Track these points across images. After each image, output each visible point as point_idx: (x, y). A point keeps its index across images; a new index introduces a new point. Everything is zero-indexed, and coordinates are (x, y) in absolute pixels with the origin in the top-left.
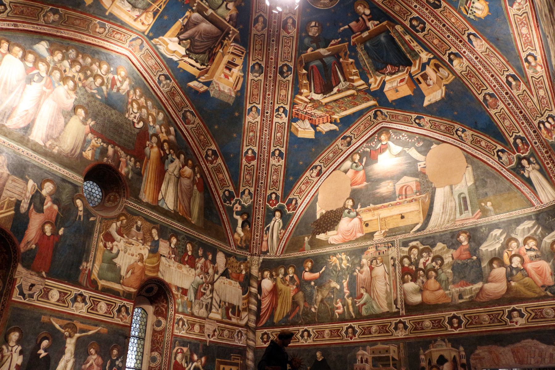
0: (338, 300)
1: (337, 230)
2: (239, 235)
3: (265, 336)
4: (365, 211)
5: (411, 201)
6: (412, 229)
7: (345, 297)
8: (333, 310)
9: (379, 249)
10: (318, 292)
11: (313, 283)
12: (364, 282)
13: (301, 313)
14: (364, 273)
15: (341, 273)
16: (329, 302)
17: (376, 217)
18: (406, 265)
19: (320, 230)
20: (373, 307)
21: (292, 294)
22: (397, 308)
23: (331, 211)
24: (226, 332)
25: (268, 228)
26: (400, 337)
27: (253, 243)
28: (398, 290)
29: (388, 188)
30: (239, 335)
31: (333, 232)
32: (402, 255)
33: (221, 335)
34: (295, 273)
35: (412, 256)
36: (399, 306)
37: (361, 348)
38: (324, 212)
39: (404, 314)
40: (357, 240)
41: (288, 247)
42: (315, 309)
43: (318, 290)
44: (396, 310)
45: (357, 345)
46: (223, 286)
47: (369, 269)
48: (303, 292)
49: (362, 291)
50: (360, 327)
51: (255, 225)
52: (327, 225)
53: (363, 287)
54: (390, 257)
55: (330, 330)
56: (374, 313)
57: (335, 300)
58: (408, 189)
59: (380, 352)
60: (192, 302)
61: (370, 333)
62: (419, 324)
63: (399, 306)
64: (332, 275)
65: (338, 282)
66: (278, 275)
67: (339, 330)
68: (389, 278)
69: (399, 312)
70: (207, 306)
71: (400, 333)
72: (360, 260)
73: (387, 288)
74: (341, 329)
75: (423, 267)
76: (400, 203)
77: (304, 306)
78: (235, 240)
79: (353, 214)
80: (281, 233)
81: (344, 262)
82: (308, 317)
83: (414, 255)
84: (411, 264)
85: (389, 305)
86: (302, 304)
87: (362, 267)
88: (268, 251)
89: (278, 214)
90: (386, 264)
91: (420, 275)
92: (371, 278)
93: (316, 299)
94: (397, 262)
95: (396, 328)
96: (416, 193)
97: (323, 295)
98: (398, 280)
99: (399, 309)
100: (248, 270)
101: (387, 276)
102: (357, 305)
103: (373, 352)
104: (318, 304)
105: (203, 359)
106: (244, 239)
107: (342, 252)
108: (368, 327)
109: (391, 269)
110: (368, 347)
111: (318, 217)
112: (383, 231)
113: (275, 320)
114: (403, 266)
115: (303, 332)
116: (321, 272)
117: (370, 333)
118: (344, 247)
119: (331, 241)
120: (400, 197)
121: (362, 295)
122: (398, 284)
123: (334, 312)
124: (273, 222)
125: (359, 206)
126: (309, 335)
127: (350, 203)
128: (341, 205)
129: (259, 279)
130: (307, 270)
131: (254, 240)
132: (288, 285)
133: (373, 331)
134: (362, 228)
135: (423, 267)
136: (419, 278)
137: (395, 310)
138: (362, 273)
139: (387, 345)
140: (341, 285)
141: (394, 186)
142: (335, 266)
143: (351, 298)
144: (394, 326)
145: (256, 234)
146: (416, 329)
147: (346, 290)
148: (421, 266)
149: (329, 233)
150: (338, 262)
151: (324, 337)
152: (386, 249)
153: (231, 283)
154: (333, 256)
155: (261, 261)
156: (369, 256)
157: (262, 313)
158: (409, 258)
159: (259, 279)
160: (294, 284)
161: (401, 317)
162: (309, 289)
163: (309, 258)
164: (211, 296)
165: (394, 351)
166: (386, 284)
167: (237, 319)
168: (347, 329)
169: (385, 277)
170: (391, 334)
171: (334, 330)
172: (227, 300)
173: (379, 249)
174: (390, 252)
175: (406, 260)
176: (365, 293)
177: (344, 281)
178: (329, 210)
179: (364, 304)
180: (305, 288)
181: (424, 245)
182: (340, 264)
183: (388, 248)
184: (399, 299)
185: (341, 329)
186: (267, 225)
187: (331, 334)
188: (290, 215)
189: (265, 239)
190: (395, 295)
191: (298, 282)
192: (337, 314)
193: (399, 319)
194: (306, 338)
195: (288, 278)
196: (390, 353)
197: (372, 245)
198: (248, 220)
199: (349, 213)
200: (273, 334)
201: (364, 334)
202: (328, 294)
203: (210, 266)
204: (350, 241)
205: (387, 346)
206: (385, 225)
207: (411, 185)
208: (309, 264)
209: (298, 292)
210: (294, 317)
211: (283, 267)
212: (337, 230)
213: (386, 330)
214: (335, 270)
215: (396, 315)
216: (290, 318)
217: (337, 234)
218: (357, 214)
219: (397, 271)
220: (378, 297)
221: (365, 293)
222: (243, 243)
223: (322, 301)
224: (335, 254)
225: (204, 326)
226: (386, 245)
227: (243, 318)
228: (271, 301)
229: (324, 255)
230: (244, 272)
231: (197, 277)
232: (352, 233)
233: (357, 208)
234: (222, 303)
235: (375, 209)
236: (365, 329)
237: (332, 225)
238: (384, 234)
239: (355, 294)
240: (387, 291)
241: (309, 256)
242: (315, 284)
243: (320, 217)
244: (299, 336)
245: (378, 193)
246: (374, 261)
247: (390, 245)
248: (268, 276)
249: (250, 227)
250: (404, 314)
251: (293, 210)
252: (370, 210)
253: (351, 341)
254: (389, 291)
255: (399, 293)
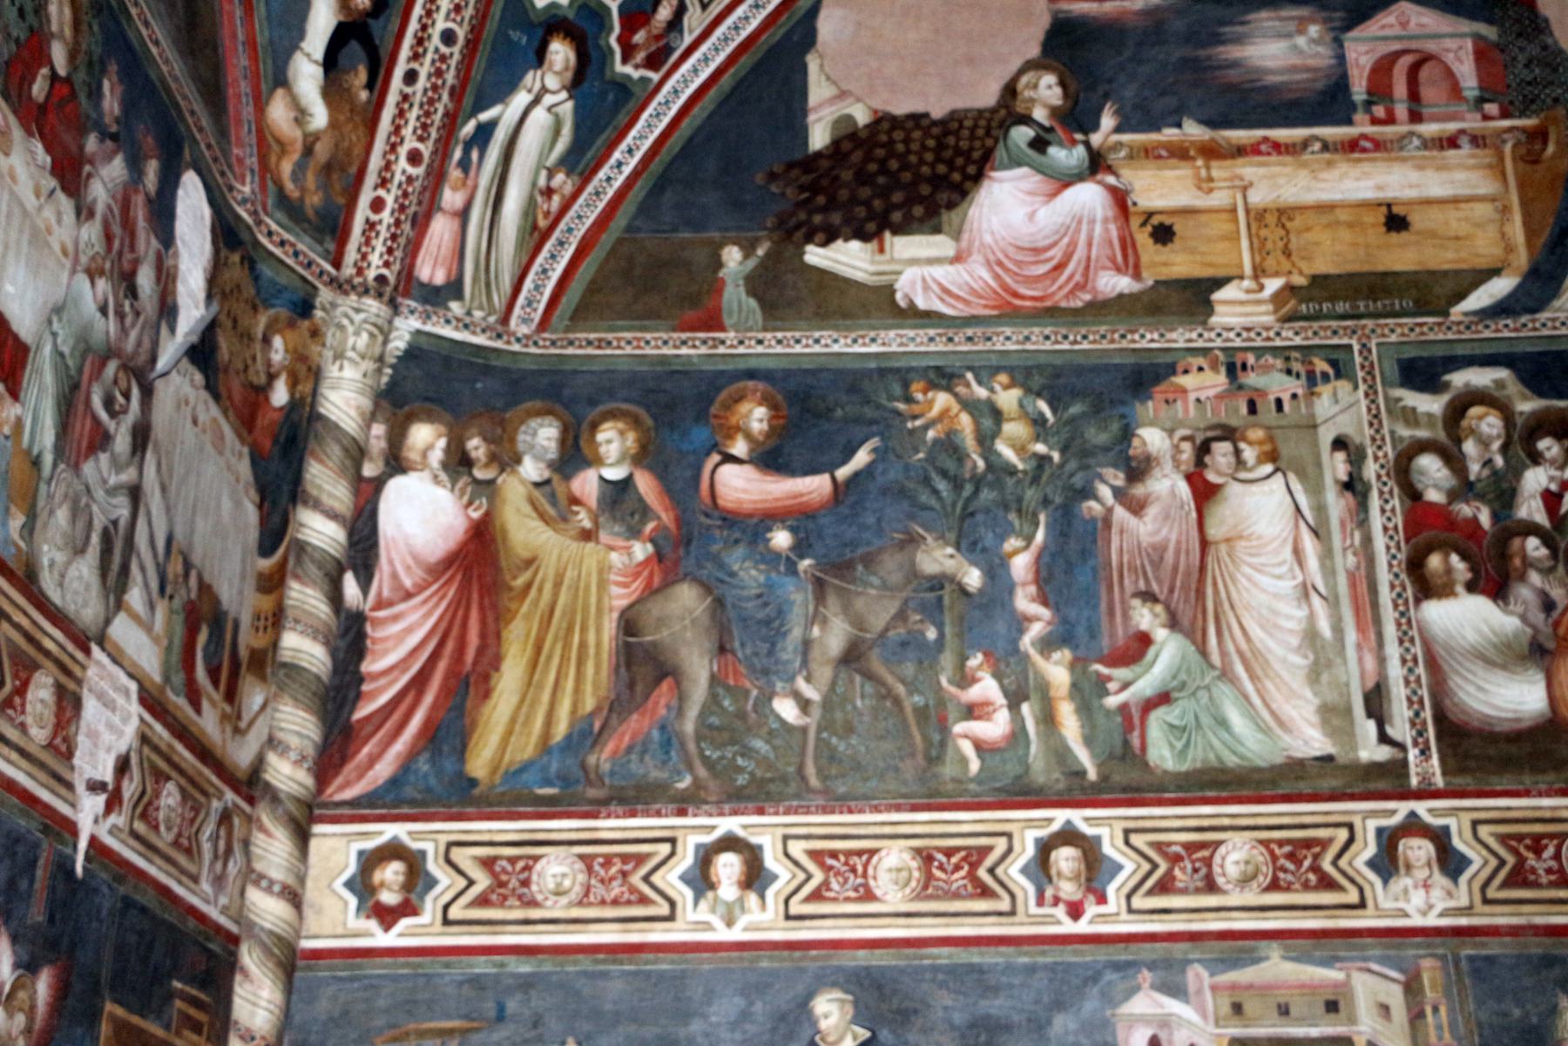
0: (975, 660)
1: (957, 236)
2: (301, 114)
3: (392, 872)
4: (1148, 153)
5: (1452, 142)
6: (1461, 296)
7: (1027, 642)
8: (936, 719)
9: (1251, 379)
10: (820, 598)
11: (781, 539)
12: (1157, 564)
13: (689, 727)
14: (1152, 511)
15: (987, 495)
16: (909, 669)
17: (1219, 198)
18: (1434, 496)
19: (836, 218)
20: (1223, 723)
21: (620, 597)
22: (1384, 738)
23: (917, 119)
24: (170, 797)
25: (485, 133)
26: (1417, 921)
27: (377, 205)
28: (1390, 631)
29: (1295, 47)
30: (222, 844)
31: (939, 245)
32: (1405, 432)
33: (145, 809)
34: (642, 457)
35: (1469, 447)
36: (1400, 729)
37: (1146, 976)
38: (862, 117)
39: (1439, 781)
40: (1102, 309)
41: (593, 288)
42: (804, 705)
43: (820, 585)
44: (1383, 753)
45: (1120, 954)
46: (189, 432)
47: (1184, 489)
48: (707, 588)
49: (1145, 618)
50: (1138, 840)
51: (411, 77)
52: (885, 193)
53: (1148, 597)
54: (1326, 436)
55: (918, 851)
56: (1231, 761)
57: (947, 660)
58: (1424, 73)
59: (1284, 1011)
60: (36, 463)
61: (1211, 887)
62: (1538, 850)
63: (1400, 729)
64: (925, 497)
65: (969, 546)
66: (507, 459)
67: (985, 851)
68: (1327, 555)
69: (1397, 769)
70: (107, 538)
71: (1418, 898)
72: (1127, 434)
73: (1312, 617)
74: (1001, 844)
75: (1541, 518)
76: (1379, 145)
77: (714, 680)
78: (266, 142)
79: (1065, 156)
80: (549, 192)
81: (1009, 428)
82: (747, 752)
83: (1484, 443)
84: (1465, 488)
85: (1334, 716)
86: (699, 668)
87: (1138, 469)
88: (454, 289)
89: (560, 52)
90: (1302, 475)
91: (1527, 563)
92: (1205, 544)
93: (807, 644)
94: (1371, 470)
95: (1387, 863)
96: (1481, 100)
97: (859, 623)
98: (1384, 577)
99: (1401, 747)
100: (305, 388)
101: (1309, 543)
102: (1112, 701)
103: (1237, 1008)
104: (825, 673)
105: (43, 986)
106: (322, 151)
107: (997, 370)
108: (1191, 847)
109: (1337, 505)
110: (1198, 976)
111: (819, 138)
112: (1273, 285)
113: (479, 763)
114: (1412, 494)
115: (706, 857)
116: (843, 473)
117: (1211, 887)
118: (1007, 340)
119: (911, 286)
120: (1379, 111)
121: (1144, 640)
122: (1385, 596)
123: (944, 729)
124: (521, 99)
125: (1107, 121)
126: (755, 877)
127: (1046, 91)
128: (986, 95)
129: (369, 470)
130: (740, 448)
131: (383, 183)
132: (587, 536)
133: (1233, 870)
134: (1127, 244)
135: (1541, 518)
136: (1522, 578)
137: (1370, 751)
138: (1137, 508)
139: (1327, 962)
140: (996, 570)
141: (1338, 43)
142: (950, 445)
143: (1064, 655)
144: (1371, 850)
145: (410, 143)
146: (1518, 877)
147: (1024, 602)
148: (1531, 509)
149: (903, 246)
150: (965, 420)
151: (869, 896)
152: (1297, 385)
153: (219, 439)
154: (932, 386)
155: (399, 343)
156: (1186, 410)
157: (363, 711)
158: (1454, 460)
159: (369, 470)
160: (634, 533)
161: (1420, 795)
162: (751, 576)
163: (751, 374)
164: (128, 476)
165: (1385, 1009)
166: (1305, 591)
167: (224, 718)
168: (1045, 849)
169: (1297, 552)
170: (1352, 896)
171: (949, 852)
172: (196, 558)
173: (1251, 379)
174: (1324, 405)
175: (1431, 467)
176: (1160, 634)
177: (1012, 543)
178: (900, 108)
179: (1163, 698)
180: (721, 566)
181: (1541, 394)
182: (985, 441)
183: (1311, 379)
184: (1398, 692)
185: (1001, 844)
186: (480, 106)
187: (929, 877)
188: (623, 88)
189: (451, 198)
190: (1370, 663)
191: (667, 518)
192: (967, 748)
193: (1403, 808)
194: (728, 889)
195: (587, 484)
196: (1352, 1020)
197: (1205, 351)
198: (375, 25)
199: (1039, 144)
200: (458, 855)
201: (1165, 886)
202: (901, 616)
203: (147, 243)
204: (1051, 314)
205: (1334, 974)
206: (1287, 253)
207: (1449, 58)
208: (757, 417)
209: (667, 584)
210: (641, 747)
211: (549, 412)
212: (957, 236)
213: (1315, 868)
214: (944, 474)
215: (1381, 785)
216: (602, 758)
217: (958, 259)
218: (1097, 164)
219: (1376, 521)
220: (1255, 662)
221: (1160, 634)
222: (311, 180)
223: (852, 657)
224: (943, 377)
225: (77, 704)
226: (1297, 366)
227: (246, 717)
228: (447, 633)
229: (867, 374)
230: (280, 395)
231: (83, 281)
232: (1060, 267)
233: (1096, 126)
234: (175, 567)
235: (1211, 152)
236: (1176, 859)
237: (921, 200)
238: (1278, 299)
239: (1093, 634)
240: (1311, 635)
241: (753, 364)
242: (801, 547)
243: (836, 143)
244: (671, 878)
245: (1235, 64)
246: (1222, 449)
247: (1321, 366)
248: (436, 456)
249: (370, 86)
250: (1439, 781)
251: (653, 62)
252: (1180, 153)
253: (1069, 927)
254: (1324, 627)
255: (1393, 651)
